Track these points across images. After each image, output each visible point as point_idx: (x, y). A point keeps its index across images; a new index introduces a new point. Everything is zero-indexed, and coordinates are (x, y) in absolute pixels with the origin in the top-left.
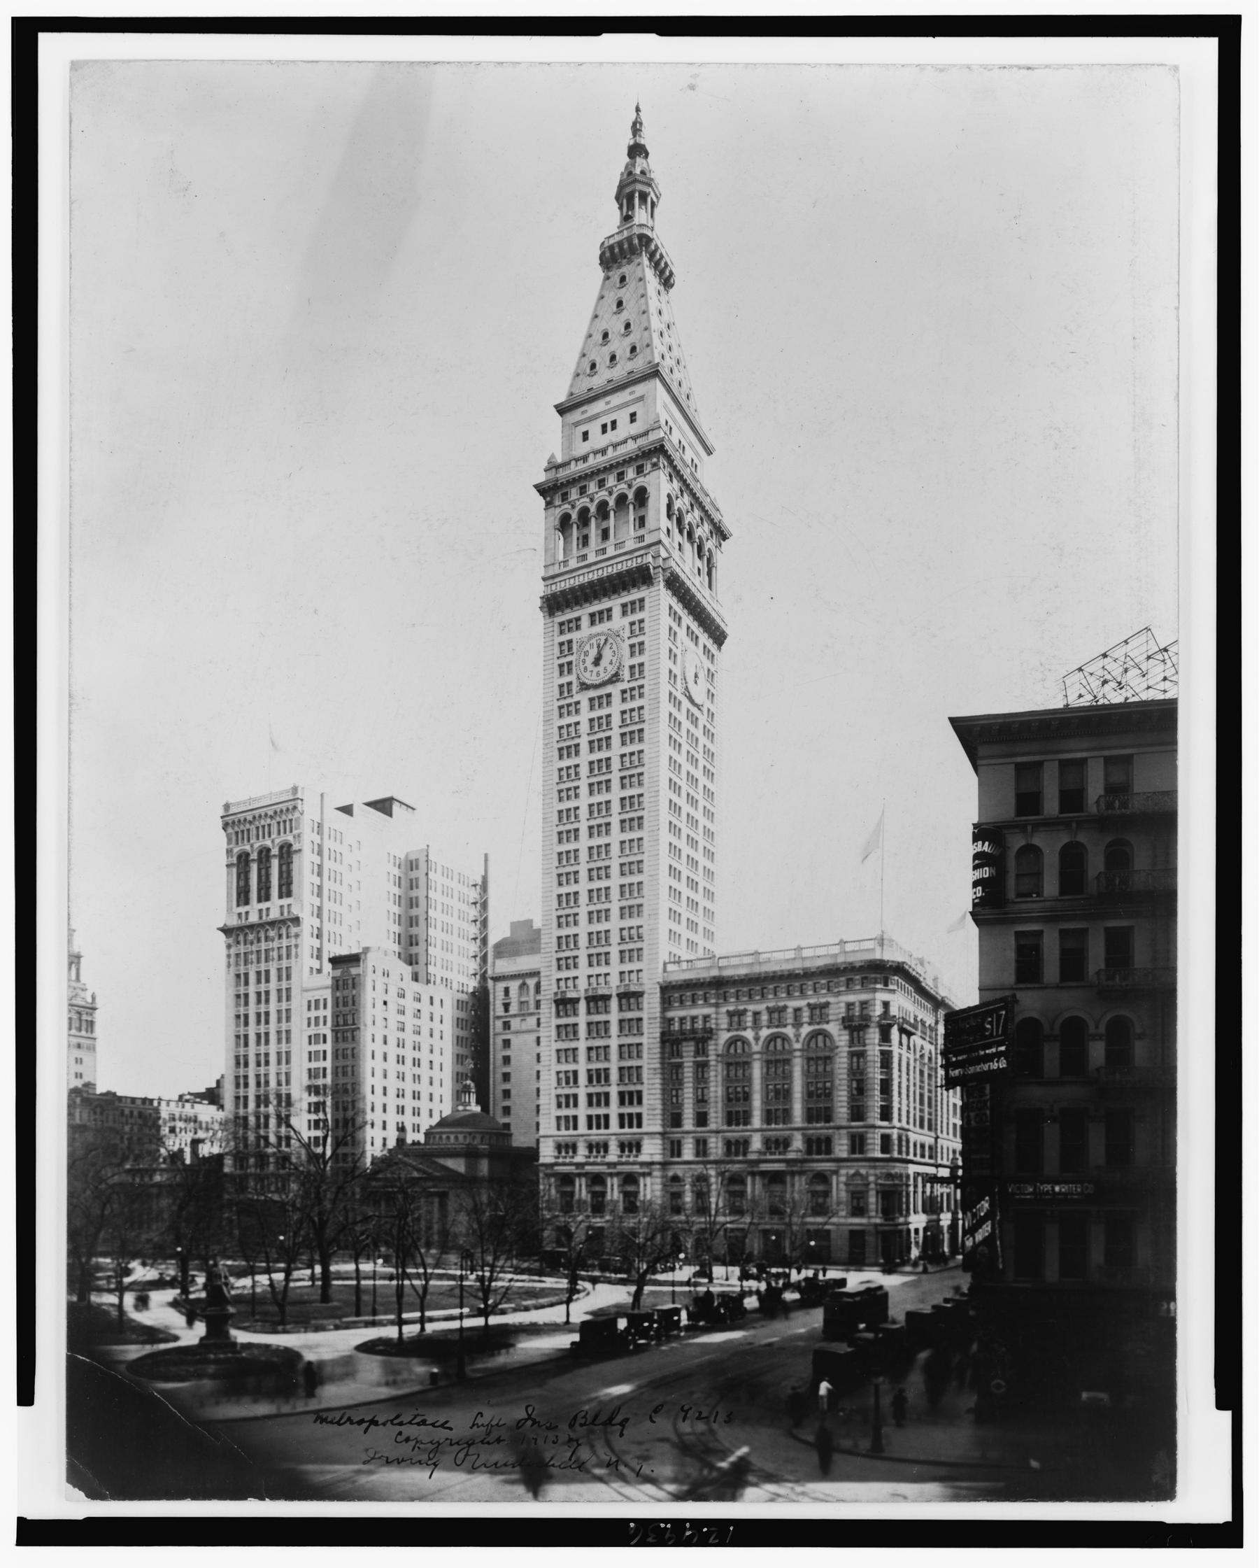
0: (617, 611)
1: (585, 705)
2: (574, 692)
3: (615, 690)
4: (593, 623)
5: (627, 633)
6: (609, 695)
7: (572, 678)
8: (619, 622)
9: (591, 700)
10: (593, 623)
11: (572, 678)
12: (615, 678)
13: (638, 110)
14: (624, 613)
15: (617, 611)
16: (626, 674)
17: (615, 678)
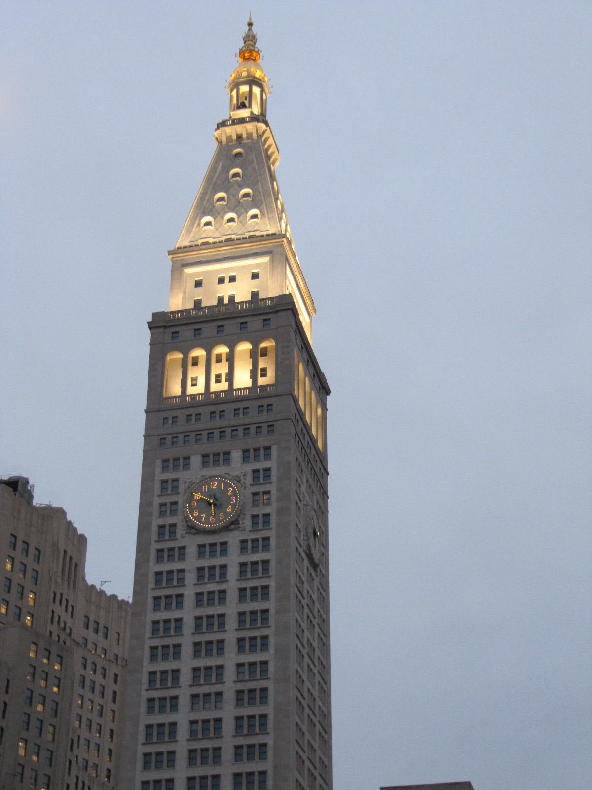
0: (236, 455)
1: (192, 550)
2: (178, 536)
3: (233, 539)
4: (205, 464)
5: (249, 480)
6: (224, 544)
7: (177, 520)
8: (237, 466)
9: (201, 546)
10: (205, 464)
11: (177, 520)
12: (233, 525)
13: (250, 24)
14: (245, 458)
15: (236, 455)
16: (247, 523)
17: (233, 525)
